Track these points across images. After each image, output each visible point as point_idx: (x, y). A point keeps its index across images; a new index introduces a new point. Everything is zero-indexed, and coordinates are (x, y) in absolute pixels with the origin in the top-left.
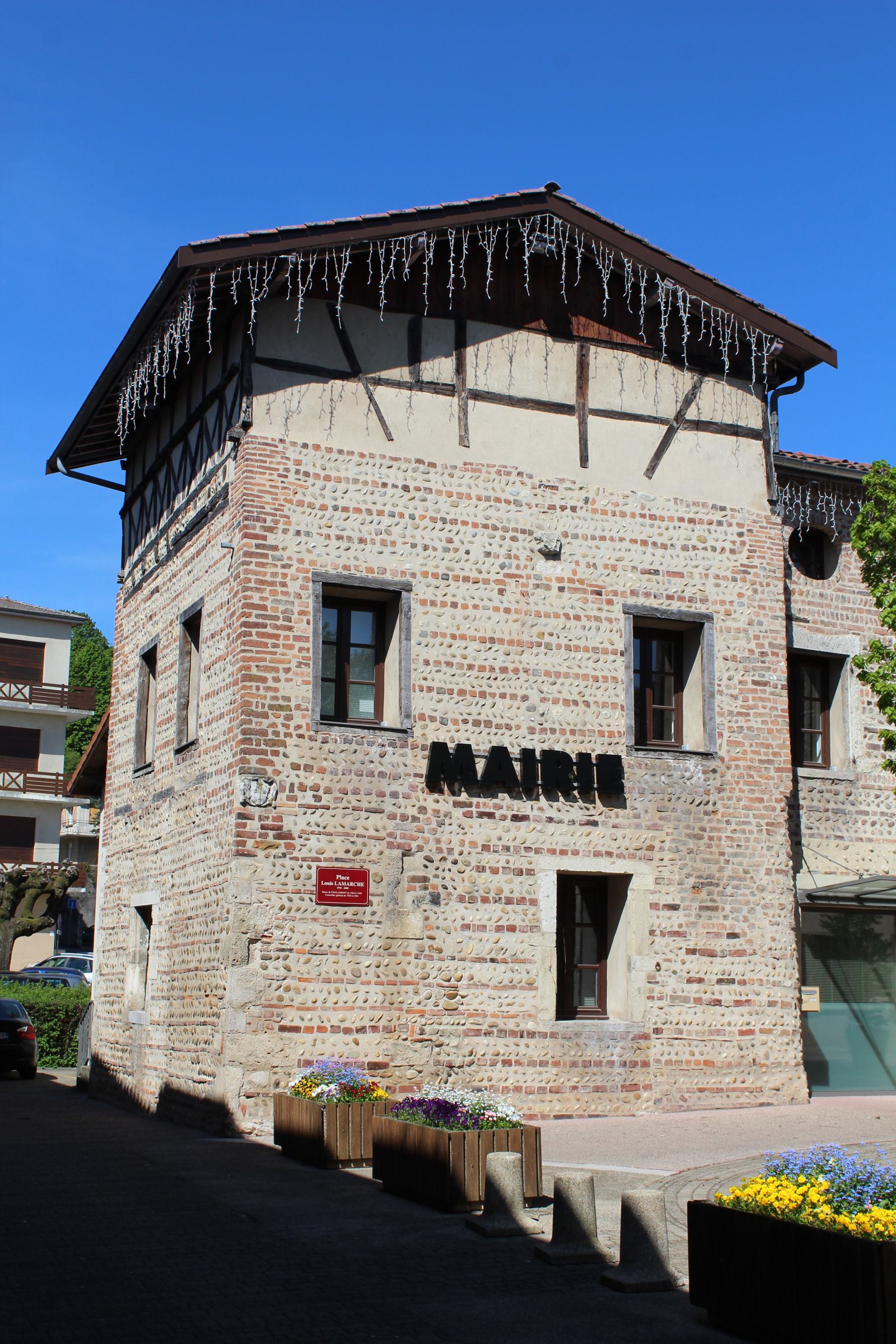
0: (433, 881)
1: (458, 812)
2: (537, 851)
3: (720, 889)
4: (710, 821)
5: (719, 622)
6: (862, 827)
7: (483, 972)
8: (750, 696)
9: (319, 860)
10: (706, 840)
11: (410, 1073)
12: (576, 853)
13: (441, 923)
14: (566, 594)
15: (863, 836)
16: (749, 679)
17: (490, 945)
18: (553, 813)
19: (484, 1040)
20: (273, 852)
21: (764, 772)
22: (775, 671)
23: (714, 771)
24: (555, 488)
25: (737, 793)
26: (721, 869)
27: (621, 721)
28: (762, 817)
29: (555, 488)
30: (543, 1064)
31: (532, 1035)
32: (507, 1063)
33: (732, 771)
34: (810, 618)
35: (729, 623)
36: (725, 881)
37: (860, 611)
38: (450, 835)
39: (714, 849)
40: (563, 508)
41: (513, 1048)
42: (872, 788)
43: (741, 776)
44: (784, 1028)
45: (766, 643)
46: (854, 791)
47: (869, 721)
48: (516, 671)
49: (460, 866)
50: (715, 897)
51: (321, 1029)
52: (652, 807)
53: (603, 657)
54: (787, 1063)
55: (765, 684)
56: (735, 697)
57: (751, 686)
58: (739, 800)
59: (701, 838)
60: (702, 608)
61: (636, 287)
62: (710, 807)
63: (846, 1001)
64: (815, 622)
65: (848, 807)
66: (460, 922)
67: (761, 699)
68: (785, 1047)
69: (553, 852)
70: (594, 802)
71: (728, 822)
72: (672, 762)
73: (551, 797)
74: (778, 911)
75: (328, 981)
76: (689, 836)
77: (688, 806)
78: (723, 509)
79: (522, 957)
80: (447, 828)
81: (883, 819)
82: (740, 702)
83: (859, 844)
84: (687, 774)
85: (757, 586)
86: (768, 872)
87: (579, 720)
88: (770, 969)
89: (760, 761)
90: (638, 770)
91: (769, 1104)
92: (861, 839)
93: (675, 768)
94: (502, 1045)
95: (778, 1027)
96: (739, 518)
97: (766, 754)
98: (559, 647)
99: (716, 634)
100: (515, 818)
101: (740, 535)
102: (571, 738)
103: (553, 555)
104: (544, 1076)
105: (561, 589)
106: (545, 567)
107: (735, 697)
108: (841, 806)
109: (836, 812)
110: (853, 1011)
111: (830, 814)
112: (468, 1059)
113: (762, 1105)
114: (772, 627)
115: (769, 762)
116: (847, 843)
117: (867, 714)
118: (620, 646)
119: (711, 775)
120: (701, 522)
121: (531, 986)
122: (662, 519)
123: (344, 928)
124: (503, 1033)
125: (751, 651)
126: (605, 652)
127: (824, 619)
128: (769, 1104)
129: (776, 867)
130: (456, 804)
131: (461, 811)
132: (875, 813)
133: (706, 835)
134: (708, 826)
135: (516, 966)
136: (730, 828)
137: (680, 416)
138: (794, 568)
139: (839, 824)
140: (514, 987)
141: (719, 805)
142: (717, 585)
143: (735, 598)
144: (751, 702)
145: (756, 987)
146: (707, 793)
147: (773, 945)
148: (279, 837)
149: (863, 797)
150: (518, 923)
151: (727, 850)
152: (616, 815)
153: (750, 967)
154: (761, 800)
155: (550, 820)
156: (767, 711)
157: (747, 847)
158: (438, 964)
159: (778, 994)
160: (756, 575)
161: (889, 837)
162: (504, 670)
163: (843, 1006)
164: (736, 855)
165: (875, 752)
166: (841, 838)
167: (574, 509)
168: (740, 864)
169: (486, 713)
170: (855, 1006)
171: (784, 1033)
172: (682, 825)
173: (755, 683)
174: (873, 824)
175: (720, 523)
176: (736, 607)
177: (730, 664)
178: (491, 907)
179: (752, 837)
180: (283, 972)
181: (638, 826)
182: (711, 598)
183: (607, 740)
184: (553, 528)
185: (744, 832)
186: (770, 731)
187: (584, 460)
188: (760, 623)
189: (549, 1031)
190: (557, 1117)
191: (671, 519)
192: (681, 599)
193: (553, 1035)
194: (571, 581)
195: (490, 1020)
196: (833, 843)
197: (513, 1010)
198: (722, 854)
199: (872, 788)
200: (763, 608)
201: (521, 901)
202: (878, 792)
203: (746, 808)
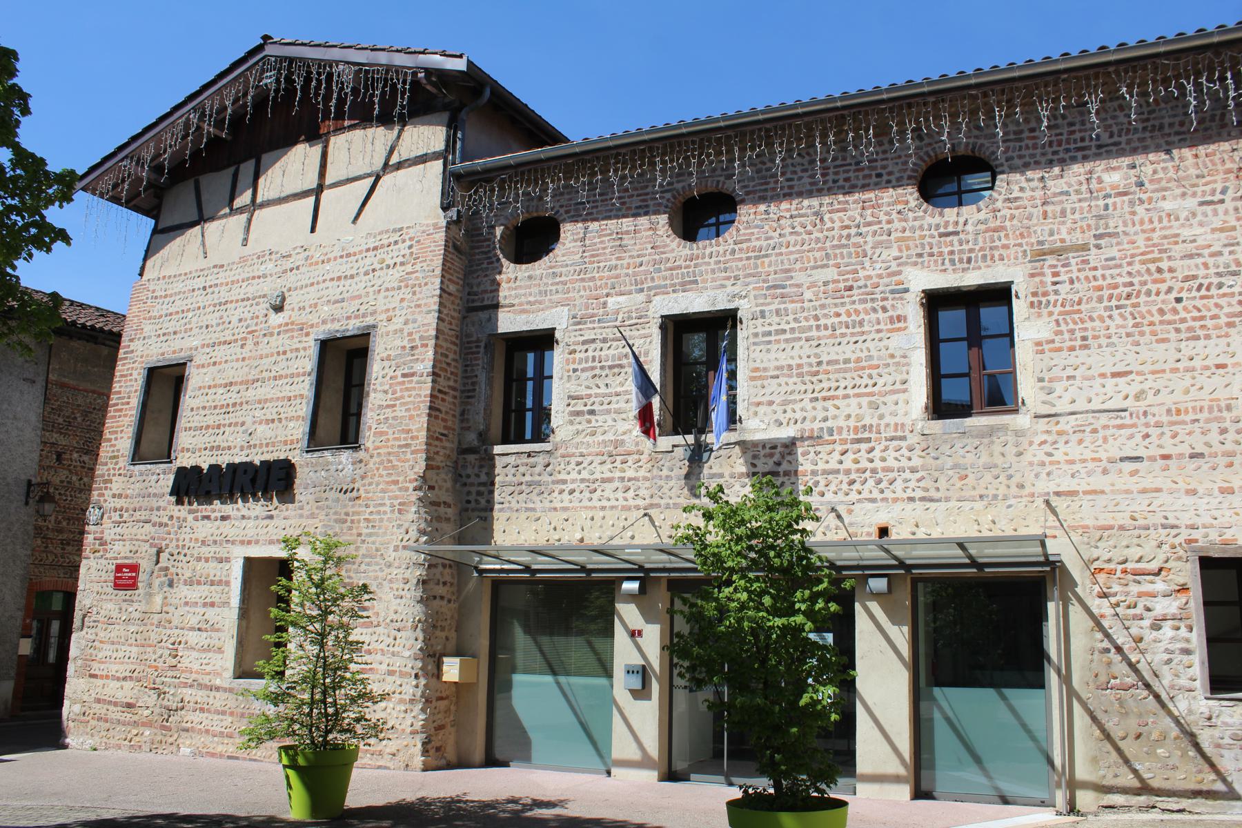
0: (172, 570)
1: (190, 517)
2: (233, 543)
3: (356, 566)
4: (353, 506)
5: (381, 330)
6: (559, 497)
7: (193, 638)
8: (398, 388)
9: (116, 558)
10: (349, 524)
11: (147, 712)
12: (257, 542)
13: (174, 601)
14: (282, 336)
15: (559, 505)
16: (399, 373)
17: (199, 617)
18: (245, 512)
19: (189, 691)
20: (97, 554)
21: (402, 456)
22: (423, 361)
23: (361, 461)
24: (290, 256)
25: (376, 479)
26: (357, 549)
27: (299, 430)
28: (396, 497)
29: (290, 256)
30: (224, 713)
31: (218, 689)
32: (202, 710)
33: (376, 459)
34: (516, 301)
35: (391, 328)
36: (359, 560)
37: (572, 281)
38: (185, 535)
39: (354, 531)
40: (291, 270)
41: (206, 699)
42: (573, 455)
43: (381, 463)
44: (403, 696)
45: (416, 336)
46: (552, 461)
47: (573, 388)
48: (241, 404)
49: (188, 558)
50: (352, 574)
51: (107, 677)
52: (311, 498)
53: (296, 380)
54: (403, 730)
55: (413, 375)
56: (386, 392)
57: (400, 379)
58: (378, 484)
59: (346, 521)
60: (369, 320)
61: (319, 82)
62: (355, 494)
63: (554, 673)
64: (521, 304)
65: (546, 478)
66: (183, 600)
67: (407, 389)
68: (403, 715)
69: (242, 542)
70: (271, 499)
71: (367, 506)
72: (330, 459)
73: (245, 500)
74: (402, 586)
75: (113, 643)
76: (336, 521)
77: (338, 494)
78: (401, 229)
79: (216, 626)
80: (184, 530)
81: (583, 486)
82: (390, 396)
83: (554, 513)
84: (340, 467)
85: (417, 289)
86: (396, 549)
87: (273, 434)
88: (391, 640)
89: (399, 446)
90: (311, 471)
91: (386, 768)
92: (555, 509)
93: (331, 463)
94: (200, 696)
95: (397, 695)
96: (412, 232)
97: (405, 439)
98: (269, 379)
99: (378, 339)
100: (224, 518)
101: (410, 247)
102: (265, 449)
103: (278, 309)
104: (225, 724)
105: (279, 334)
106: (276, 319)
107: (386, 392)
108: (537, 478)
109: (529, 484)
110: (558, 683)
111: (524, 487)
112: (180, 705)
113: (379, 767)
114: (426, 321)
115: (407, 446)
116: (538, 514)
117: (573, 382)
118: (309, 369)
119: (358, 465)
120: (382, 246)
121: (220, 650)
122: (355, 254)
123: (124, 605)
124: (201, 686)
125: (403, 348)
126: (298, 375)
127: (532, 299)
128: (386, 768)
129: (404, 543)
130: (190, 512)
131: (192, 516)
132: (573, 481)
133: (349, 519)
134: (351, 510)
135: (213, 634)
136: (368, 510)
137: (386, 165)
138: (503, 260)
139: (533, 496)
140: (209, 651)
141: (362, 492)
142: (386, 297)
143: (397, 304)
144: (398, 394)
145: (379, 657)
146: (353, 481)
147: (395, 617)
148: (101, 545)
149: (562, 466)
150: (217, 600)
151: (365, 531)
152: (289, 510)
153: (375, 637)
154: (396, 482)
155: (243, 517)
156: (412, 399)
157: (380, 528)
158: (169, 632)
159: (398, 663)
160: (417, 278)
161: (589, 504)
162: (234, 405)
163: (549, 679)
164: (370, 535)
165: (578, 419)
166: (533, 510)
167: (298, 268)
168: (374, 543)
169: (219, 440)
170: (562, 679)
171: (401, 701)
172: (332, 511)
173: (404, 375)
174: (572, 492)
175: (396, 243)
176: (398, 312)
177: (386, 363)
178: (203, 587)
179: (385, 517)
180: (93, 637)
181: (301, 516)
182: (379, 310)
183: (289, 447)
184: (270, 288)
185: (379, 513)
186: (411, 417)
187: (313, 230)
188: (415, 321)
189: (227, 685)
190: (230, 757)
191: (361, 252)
192: (357, 317)
193: (231, 690)
194: (287, 324)
195: (194, 676)
196: (523, 515)
197: (208, 669)
198: (360, 535)
199: (573, 455)
200: (419, 306)
201: (220, 583)
202: (580, 459)
203: (383, 491)
